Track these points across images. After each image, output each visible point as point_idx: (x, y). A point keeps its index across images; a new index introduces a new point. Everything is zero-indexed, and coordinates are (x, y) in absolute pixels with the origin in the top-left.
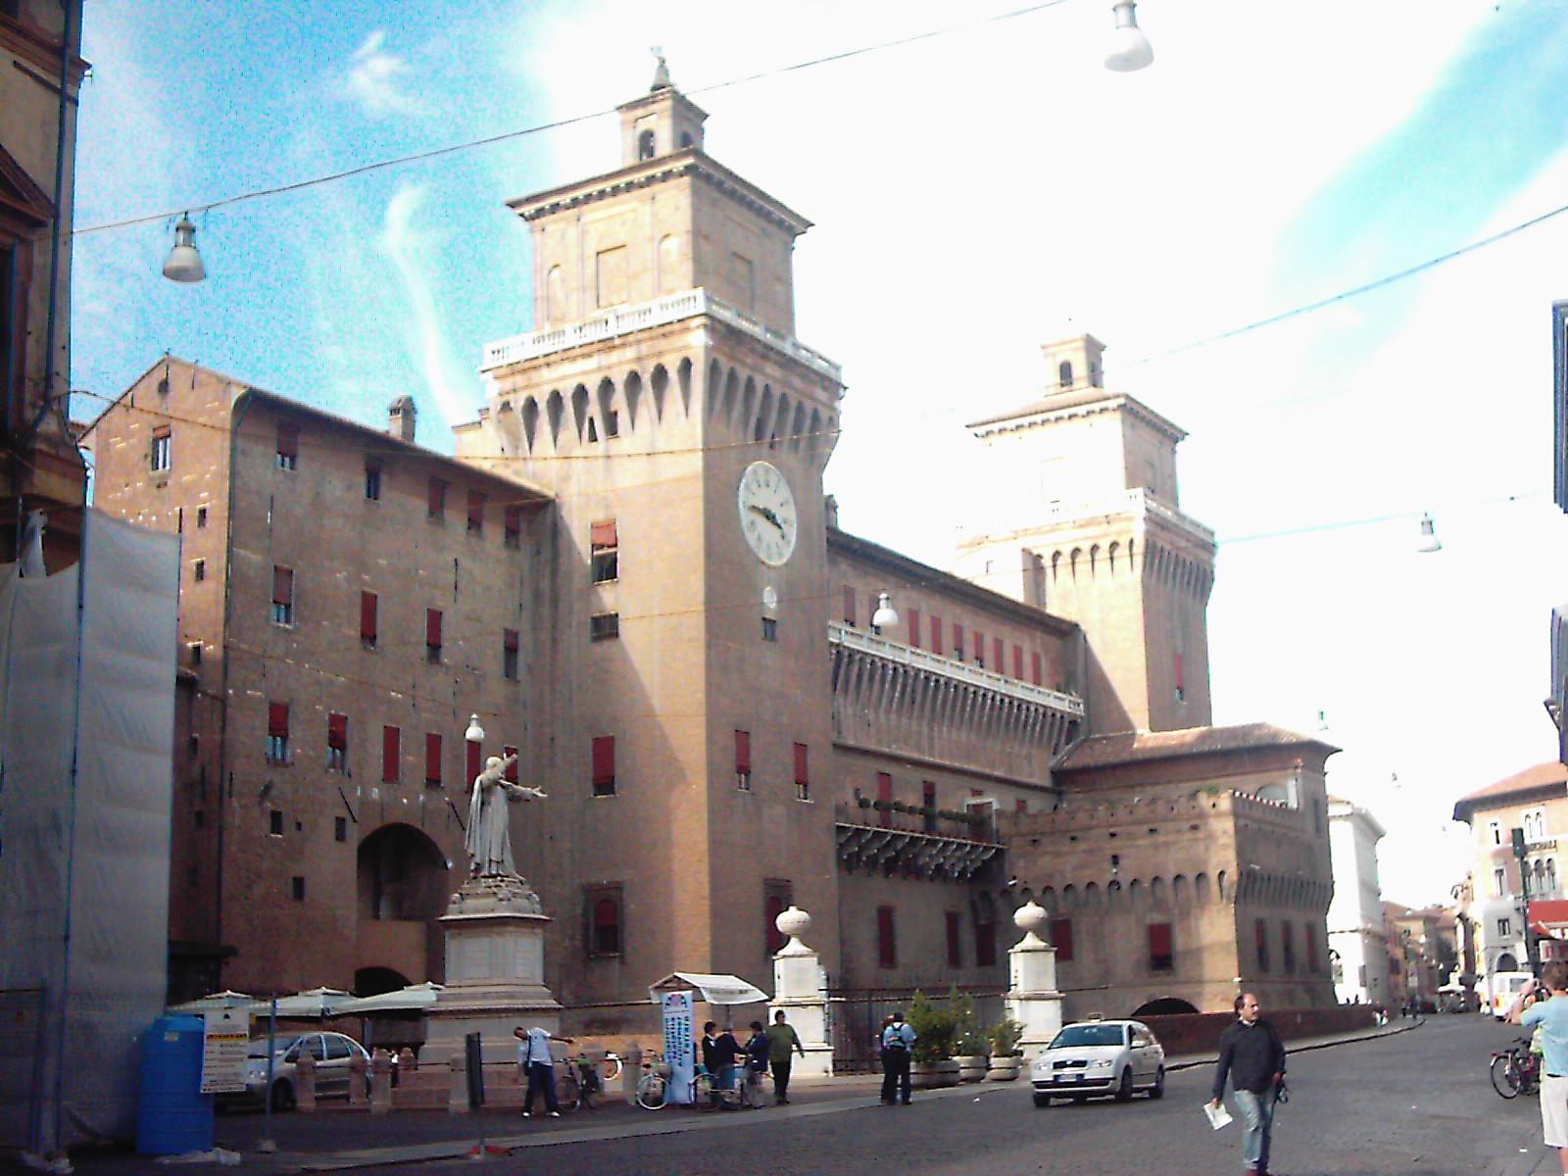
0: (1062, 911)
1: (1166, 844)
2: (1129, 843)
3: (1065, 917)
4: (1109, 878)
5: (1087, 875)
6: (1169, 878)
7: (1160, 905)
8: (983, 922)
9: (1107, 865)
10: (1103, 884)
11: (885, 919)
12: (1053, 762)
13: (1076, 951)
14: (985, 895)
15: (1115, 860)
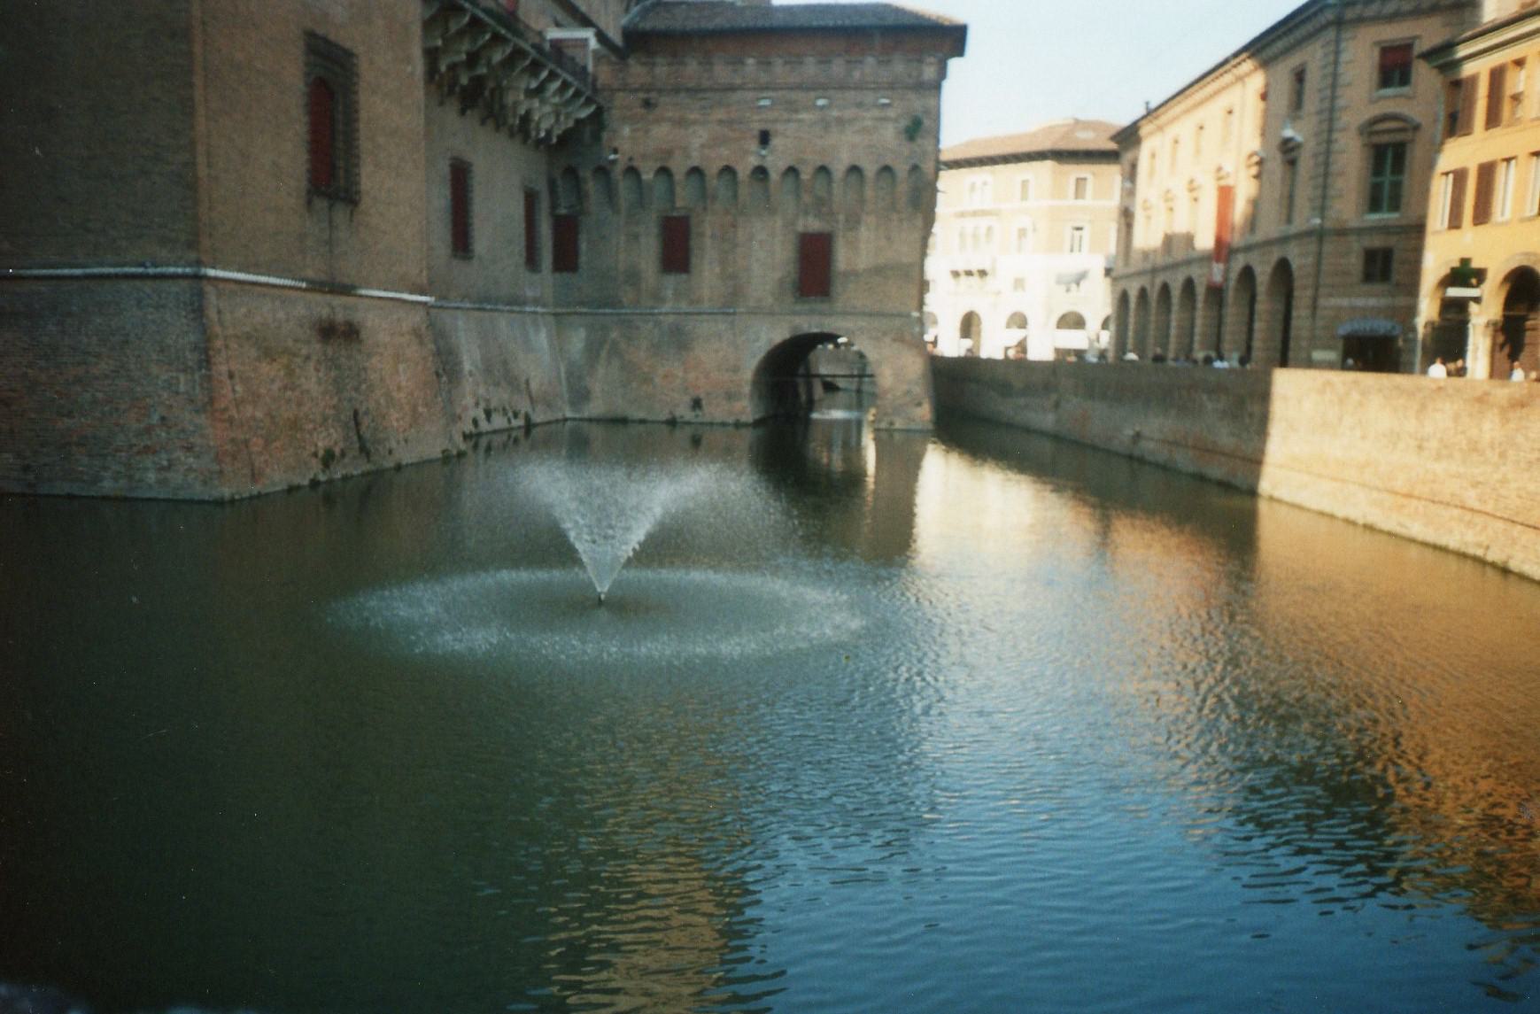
0: (679, 204)
1: (840, 121)
2: (786, 116)
3: (682, 213)
4: (753, 161)
5: (724, 155)
6: (839, 169)
7: (822, 205)
8: (563, 211)
9: (753, 145)
10: (743, 171)
11: (460, 177)
12: (624, 21)
13: (694, 260)
14: (571, 172)
15: (764, 138)
